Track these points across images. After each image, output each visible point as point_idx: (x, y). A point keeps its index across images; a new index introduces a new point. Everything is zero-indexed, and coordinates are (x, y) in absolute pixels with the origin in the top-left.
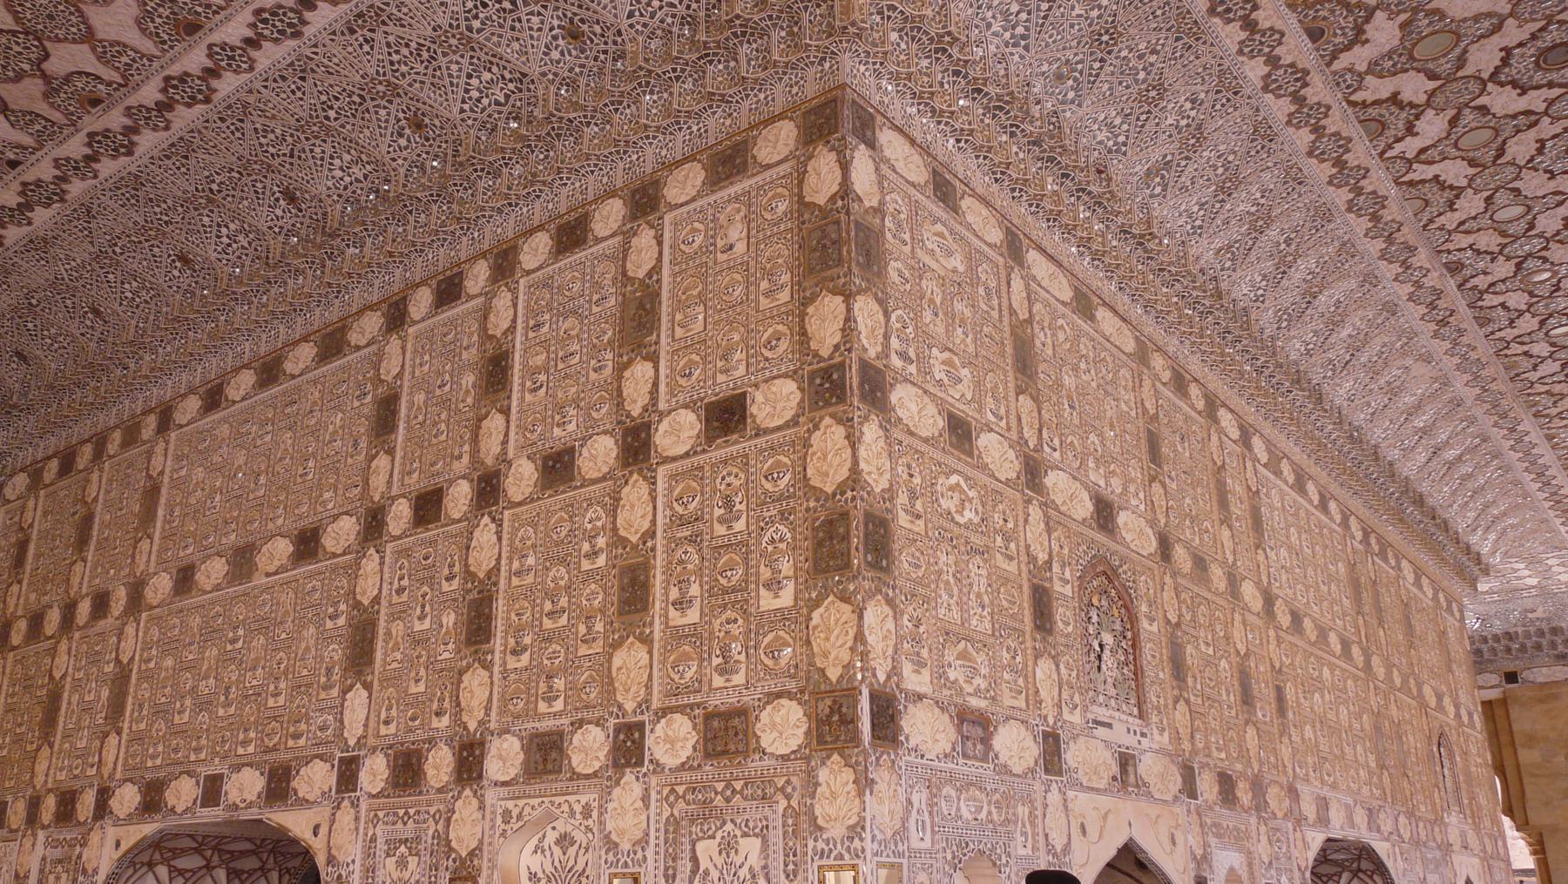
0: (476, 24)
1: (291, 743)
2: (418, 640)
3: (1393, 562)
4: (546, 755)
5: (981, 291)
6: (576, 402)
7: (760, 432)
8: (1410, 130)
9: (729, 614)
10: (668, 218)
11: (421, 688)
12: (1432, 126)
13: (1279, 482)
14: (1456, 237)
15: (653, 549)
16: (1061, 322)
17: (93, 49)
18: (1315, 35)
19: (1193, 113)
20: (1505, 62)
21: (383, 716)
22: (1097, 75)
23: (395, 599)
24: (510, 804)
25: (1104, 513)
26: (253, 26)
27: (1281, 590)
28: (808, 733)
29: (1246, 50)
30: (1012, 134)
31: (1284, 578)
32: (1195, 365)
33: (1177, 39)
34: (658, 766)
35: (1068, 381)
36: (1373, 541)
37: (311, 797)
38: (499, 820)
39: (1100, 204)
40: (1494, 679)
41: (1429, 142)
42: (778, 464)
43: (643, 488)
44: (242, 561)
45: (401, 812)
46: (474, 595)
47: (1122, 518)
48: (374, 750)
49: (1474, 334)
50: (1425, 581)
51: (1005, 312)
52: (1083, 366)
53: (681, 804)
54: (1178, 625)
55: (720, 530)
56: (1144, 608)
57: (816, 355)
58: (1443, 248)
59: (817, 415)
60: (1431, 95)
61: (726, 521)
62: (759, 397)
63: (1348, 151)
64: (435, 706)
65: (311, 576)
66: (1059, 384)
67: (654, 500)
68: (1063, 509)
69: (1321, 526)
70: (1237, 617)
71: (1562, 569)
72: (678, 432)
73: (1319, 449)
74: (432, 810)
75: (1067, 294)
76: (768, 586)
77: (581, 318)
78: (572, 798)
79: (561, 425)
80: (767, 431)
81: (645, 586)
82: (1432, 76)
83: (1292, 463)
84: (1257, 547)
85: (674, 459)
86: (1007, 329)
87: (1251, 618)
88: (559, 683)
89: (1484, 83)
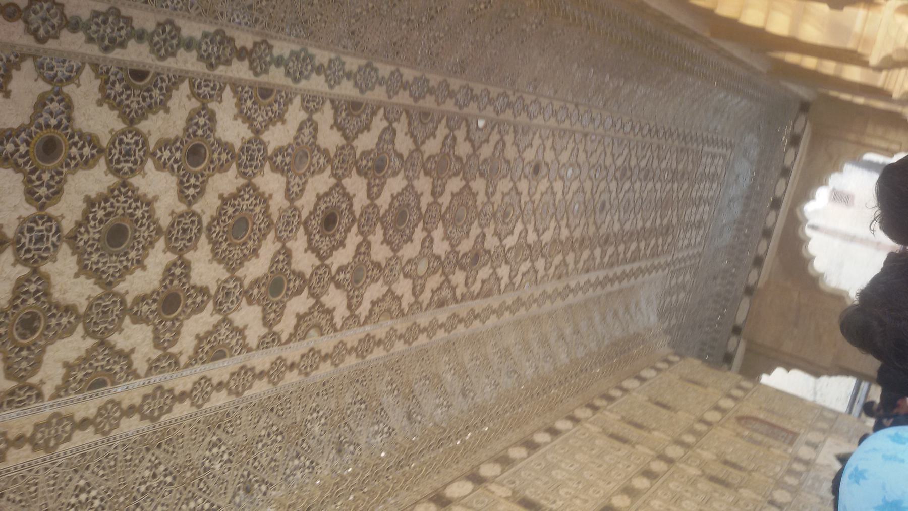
13: (519, 465)
18: (219, 355)
19: (223, 448)
29: (200, 402)
40: (733, 340)
41: (345, 302)
49: (494, 302)
50: (646, 373)
60: (312, 295)
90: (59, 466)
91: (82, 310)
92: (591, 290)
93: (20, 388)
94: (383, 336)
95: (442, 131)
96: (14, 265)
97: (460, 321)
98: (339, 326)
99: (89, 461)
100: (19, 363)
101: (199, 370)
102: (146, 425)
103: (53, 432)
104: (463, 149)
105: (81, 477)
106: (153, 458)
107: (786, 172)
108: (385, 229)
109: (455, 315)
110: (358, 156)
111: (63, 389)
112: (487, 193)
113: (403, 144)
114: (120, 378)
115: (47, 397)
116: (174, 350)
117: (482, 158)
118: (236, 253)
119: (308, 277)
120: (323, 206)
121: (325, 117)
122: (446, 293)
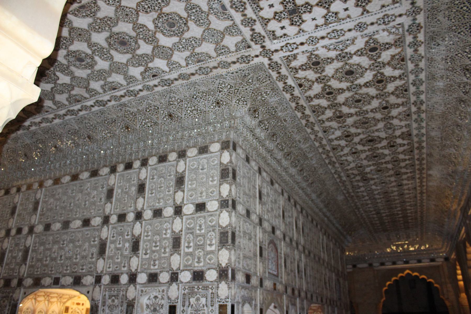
0: (148, 110)
1: (81, 271)
2: (118, 249)
4: (153, 278)
6: (163, 198)
7: (208, 212)
9: (200, 250)
10: (188, 159)
11: (119, 260)
15: (182, 234)
17: (53, 102)
21: (108, 266)
23: (112, 239)
24: (143, 289)
26: (95, 103)
28: (217, 277)
34: (182, 282)
37: (87, 284)
38: (140, 292)
40: (351, 266)
42: (212, 219)
43: (180, 220)
44: (66, 224)
45: (113, 289)
46: (135, 240)
48: (105, 274)
53: (187, 290)
55: (198, 232)
57: (222, 197)
59: (222, 210)
61: (200, 230)
62: (209, 204)
64: (123, 265)
65: (87, 230)
67: (182, 223)
72: (189, 209)
74: (122, 289)
76: (209, 245)
77: (165, 179)
78: (159, 288)
79: (159, 203)
80: (210, 212)
81: (180, 243)
85: (188, 215)
88: (157, 262)
107: (419, 261)
120: (376, 138)
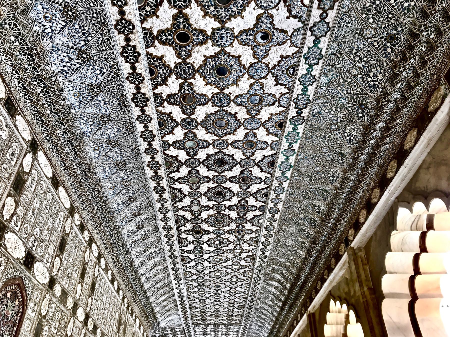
3: (134, 318)
5: (10, 151)
8: (178, 170)
12: (184, 171)
14: (181, 211)
16: (42, 182)
18: (160, 124)
20: (207, 158)
22: (88, 102)
25: (29, 260)
27: (94, 317)
29: (139, 119)
30: (49, 105)
31: (96, 311)
32: (89, 224)
33: (119, 104)
35: (36, 204)
36: (130, 309)
39: (75, 150)
41: (182, 176)
47: (36, 265)
49: (176, 246)
50: (142, 327)
51: (18, 165)
52: (45, 202)
54: (45, 316)
56: (31, 305)
58: (176, 213)
60: (186, 161)
63: (159, 169)
66: (31, 203)
68: (9, 250)
69: (115, 298)
70: (72, 321)
71: (179, 333)
73: (122, 271)
75: (50, 175)
82: (188, 154)
83: (112, 273)
84: (90, 296)
86: (16, 171)
87: (77, 322)
89: (200, 163)
90: (114, 59)
91: (188, 60)
92: (178, 291)
93: (153, 38)
94: (164, 197)
95: (258, 204)
96: (212, 28)
97: (168, 232)
98: (170, 176)
99: (115, 72)
100: (165, 35)
101: (154, 116)
102: (130, 97)
103: (131, 54)
104: (250, 215)
105: (107, 70)
106: (114, 102)
108: (215, 187)
109: (171, 228)
110: (249, 169)
111: (150, 56)
112: (229, 230)
113: (253, 189)
114: (154, 82)
115: (147, 50)
116: (166, 104)
117: (245, 225)
118: (210, 124)
119: (195, 157)
121: (268, 152)
122: (182, 222)
